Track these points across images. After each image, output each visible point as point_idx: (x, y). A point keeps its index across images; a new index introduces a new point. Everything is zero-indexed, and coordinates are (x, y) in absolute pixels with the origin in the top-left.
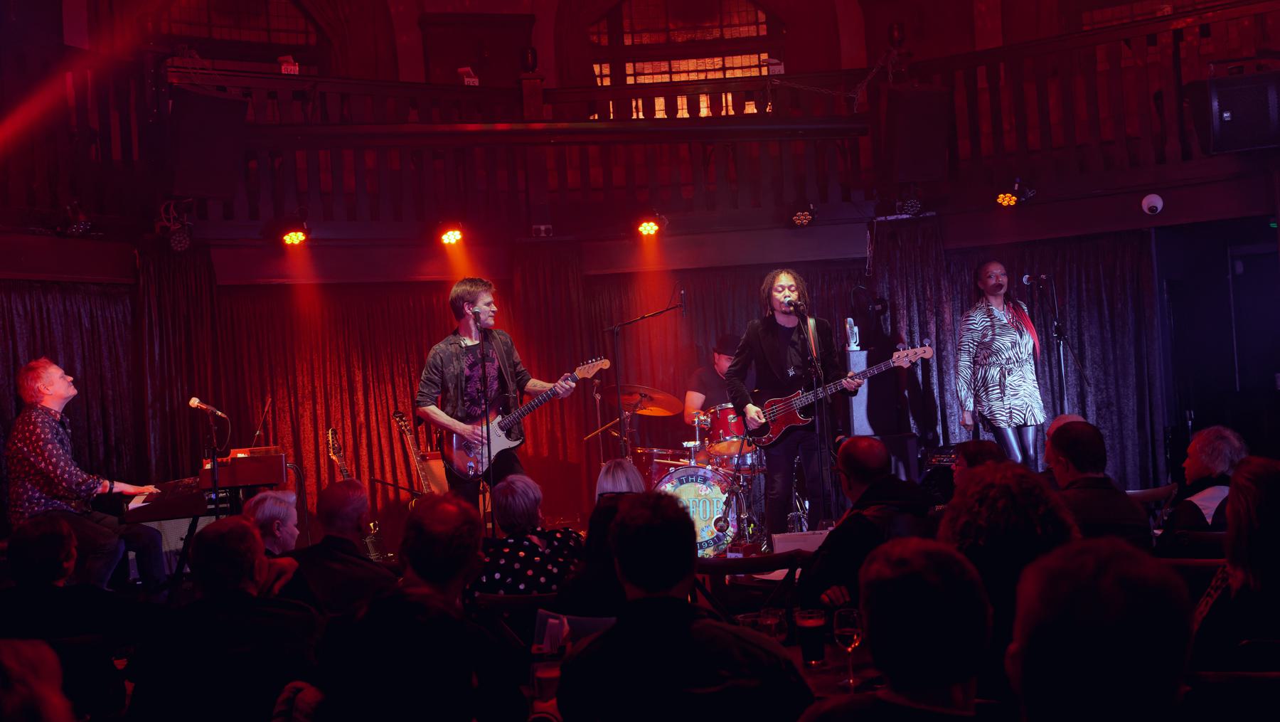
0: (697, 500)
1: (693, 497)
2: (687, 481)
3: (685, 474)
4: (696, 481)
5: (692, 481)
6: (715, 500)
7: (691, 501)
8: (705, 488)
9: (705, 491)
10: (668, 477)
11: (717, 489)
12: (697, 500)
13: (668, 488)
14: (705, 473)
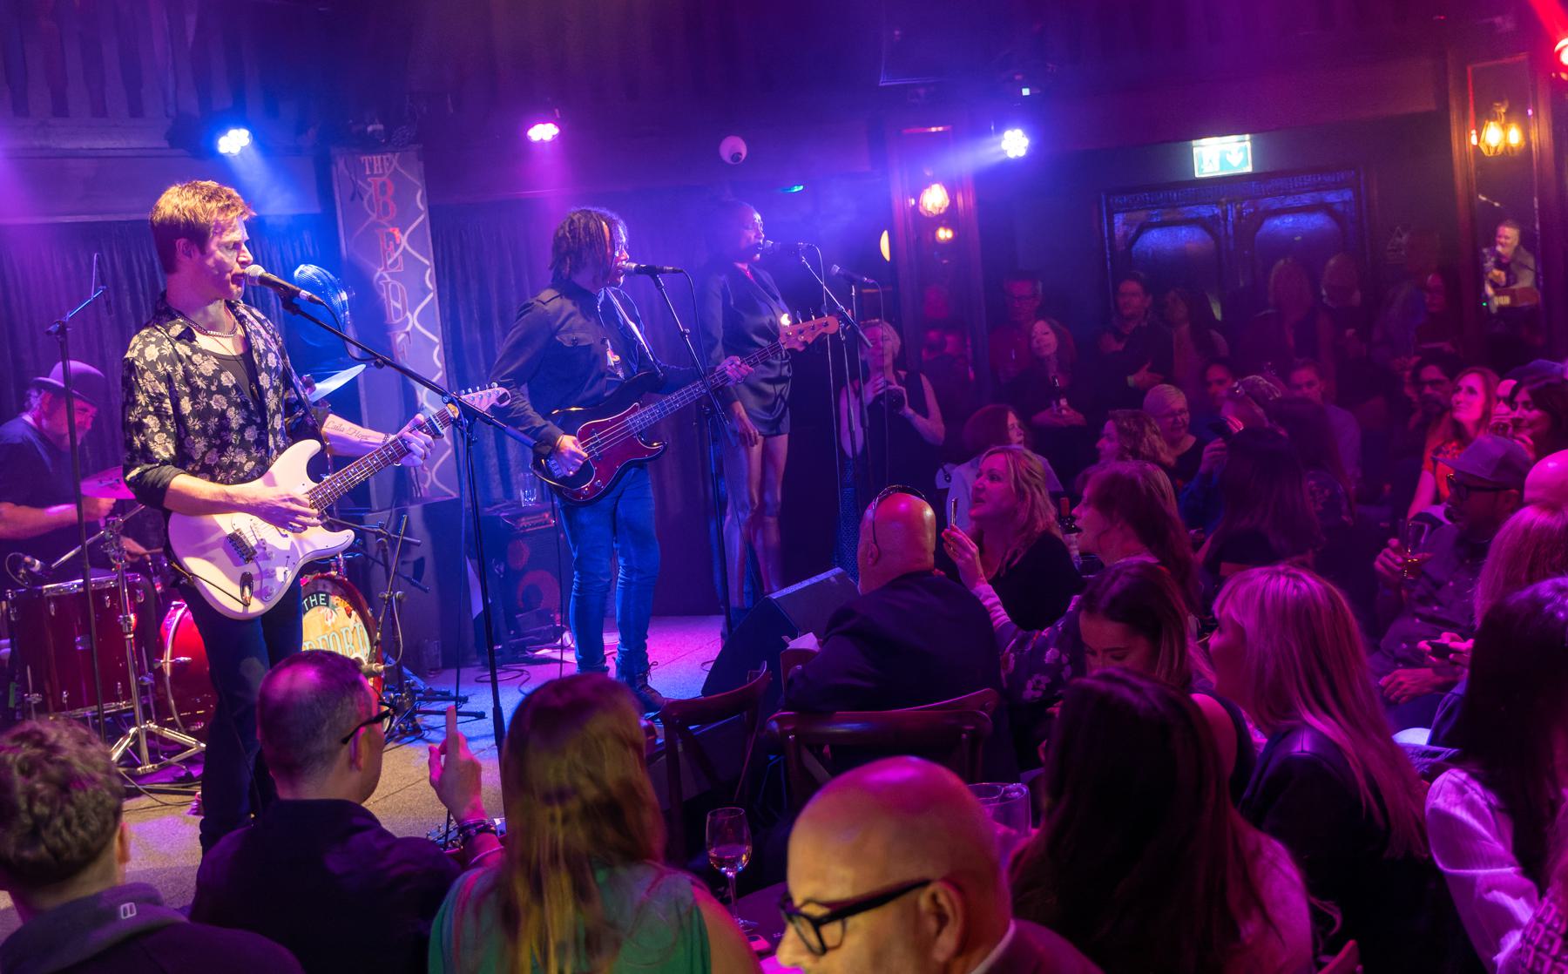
0: (326, 637)
2: (310, 608)
4: (319, 604)
5: (315, 605)
6: (343, 631)
7: (320, 640)
8: (329, 615)
9: (331, 618)
12: (326, 637)
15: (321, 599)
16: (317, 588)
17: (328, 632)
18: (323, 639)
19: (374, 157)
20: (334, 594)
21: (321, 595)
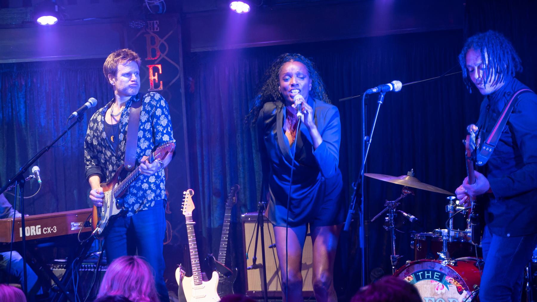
0: (433, 300)
1: (429, 296)
2: (423, 278)
4: (432, 278)
5: (428, 277)
9: (441, 289)
10: (405, 271)
11: (453, 287)
12: (433, 300)
13: (409, 279)
14: (441, 268)
15: (435, 275)
16: (433, 268)
17: (436, 297)
18: (431, 300)
21: (436, 273)
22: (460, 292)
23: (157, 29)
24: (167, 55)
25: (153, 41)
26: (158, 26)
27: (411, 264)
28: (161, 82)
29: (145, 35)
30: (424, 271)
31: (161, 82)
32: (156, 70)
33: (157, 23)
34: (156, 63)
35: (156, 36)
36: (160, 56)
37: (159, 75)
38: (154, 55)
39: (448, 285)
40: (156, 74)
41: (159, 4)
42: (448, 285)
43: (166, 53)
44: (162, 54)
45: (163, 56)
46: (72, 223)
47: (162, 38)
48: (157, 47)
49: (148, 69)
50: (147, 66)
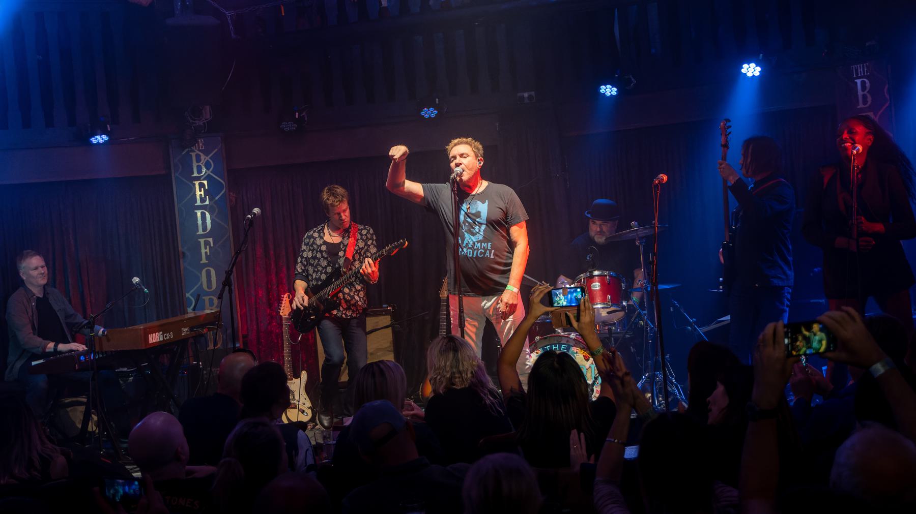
3: (547, 344)
14: (567, 341)
15: (562, 347)
19: (859, 66)
20: (574, 346)
21: (562, 345)
22: (587, 360)
23: (202, 147)
24: (212, 172)
25: (198, 160)
26: (203, 144)
27: (540, 339)
28: (207, 197)
29: (191, 153)
30: (551, 345)
31: (207, 197)
32: (202, 185)
33: (201, 141)
34: (202, 179)
35: (200, 153)
36: (206, 172)
37: (205, 190)
38: (200, 171)
39: (575, 355)
40: (202, 189)
41: (202, 124)
42: (575, 355)
43: (211, 170)
44: (207, 171)
45: (209, 172)
46: (183, 329)
47: (207, 156)
48: (202, 164)
49: (195, 184)
50: (196, 182)
